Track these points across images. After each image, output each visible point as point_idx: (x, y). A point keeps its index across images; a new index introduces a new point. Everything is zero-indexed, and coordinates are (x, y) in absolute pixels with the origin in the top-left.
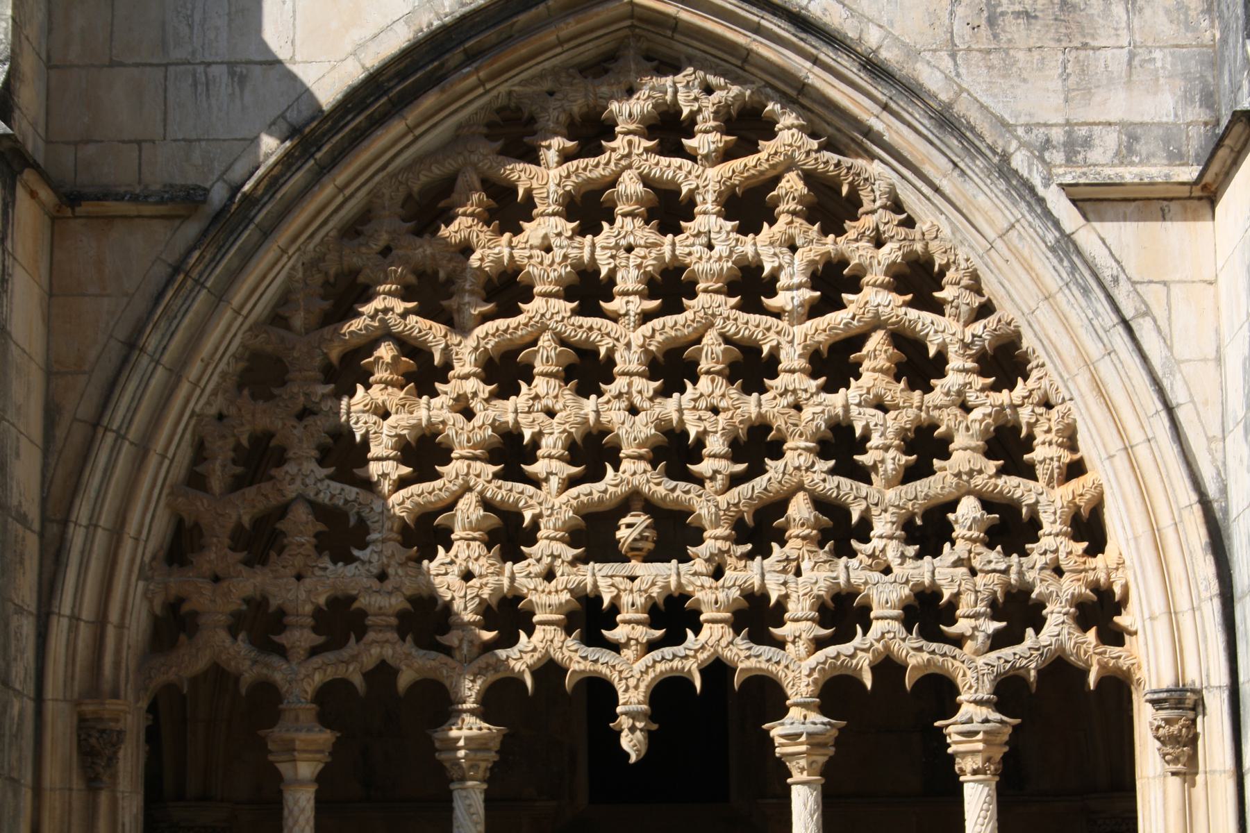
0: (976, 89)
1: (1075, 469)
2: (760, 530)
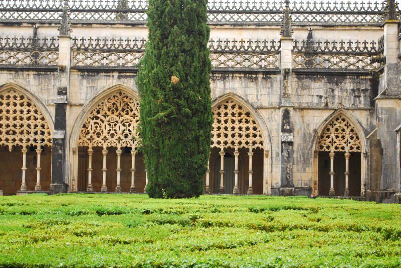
0: (40, 96)
1: (48, 128)
2: (21, 133)
